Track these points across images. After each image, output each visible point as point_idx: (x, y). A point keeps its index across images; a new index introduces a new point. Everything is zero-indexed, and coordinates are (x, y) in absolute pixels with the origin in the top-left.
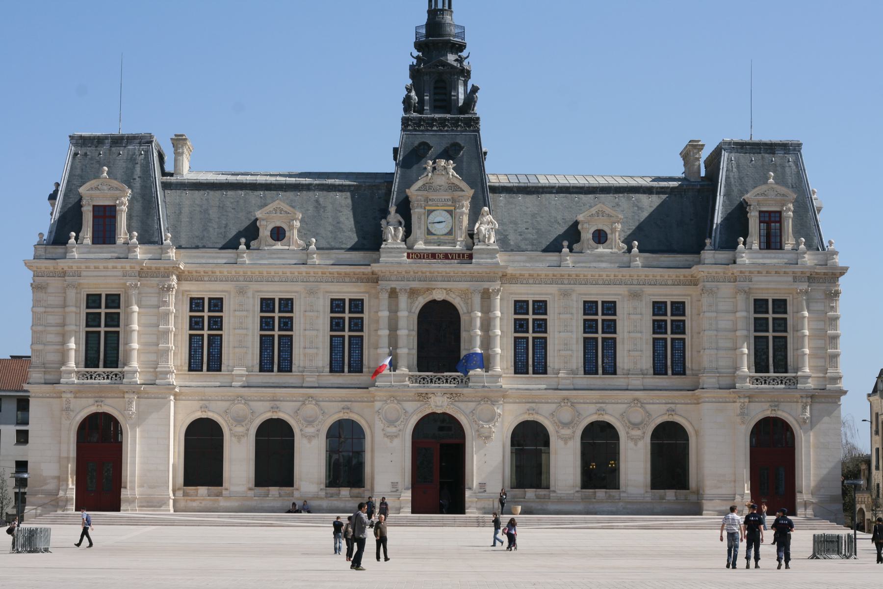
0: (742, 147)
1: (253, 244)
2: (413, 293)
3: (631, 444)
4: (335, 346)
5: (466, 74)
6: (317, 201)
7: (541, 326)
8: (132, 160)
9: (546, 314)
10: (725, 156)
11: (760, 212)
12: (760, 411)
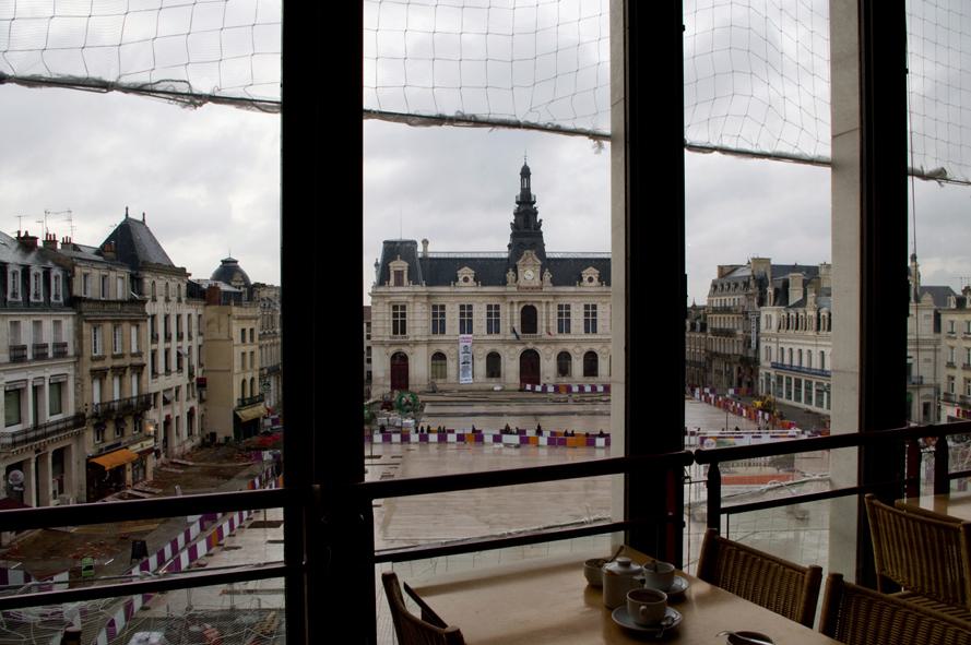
2: (519, 303)
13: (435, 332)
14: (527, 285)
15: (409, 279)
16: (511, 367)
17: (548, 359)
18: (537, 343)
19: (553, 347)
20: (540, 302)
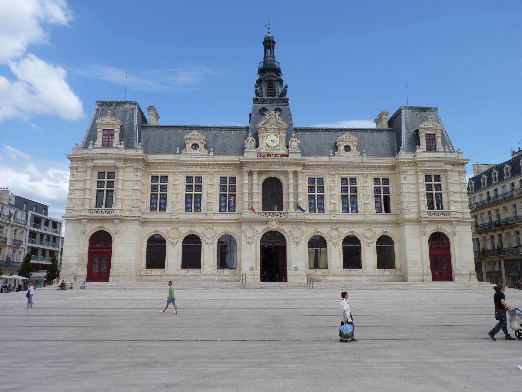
0: (410, 108)
1: (183, 151)
2: (260, 173)
3: (367, 247)
4: (222, 198)
5: (281, 82)
6: (214, 134)
7: (321, 189)
8: (126, 112)
9: (323, 184)
10: (403, 112)
11: (426, 134)
12: (431, 230)
13: (153, 208)
14: (269, 152)
15: (121, 140)
16: (249, 256)
17: (297, 243)
18: (282, 222)
19: (304, 228)
20: (286, 173)
